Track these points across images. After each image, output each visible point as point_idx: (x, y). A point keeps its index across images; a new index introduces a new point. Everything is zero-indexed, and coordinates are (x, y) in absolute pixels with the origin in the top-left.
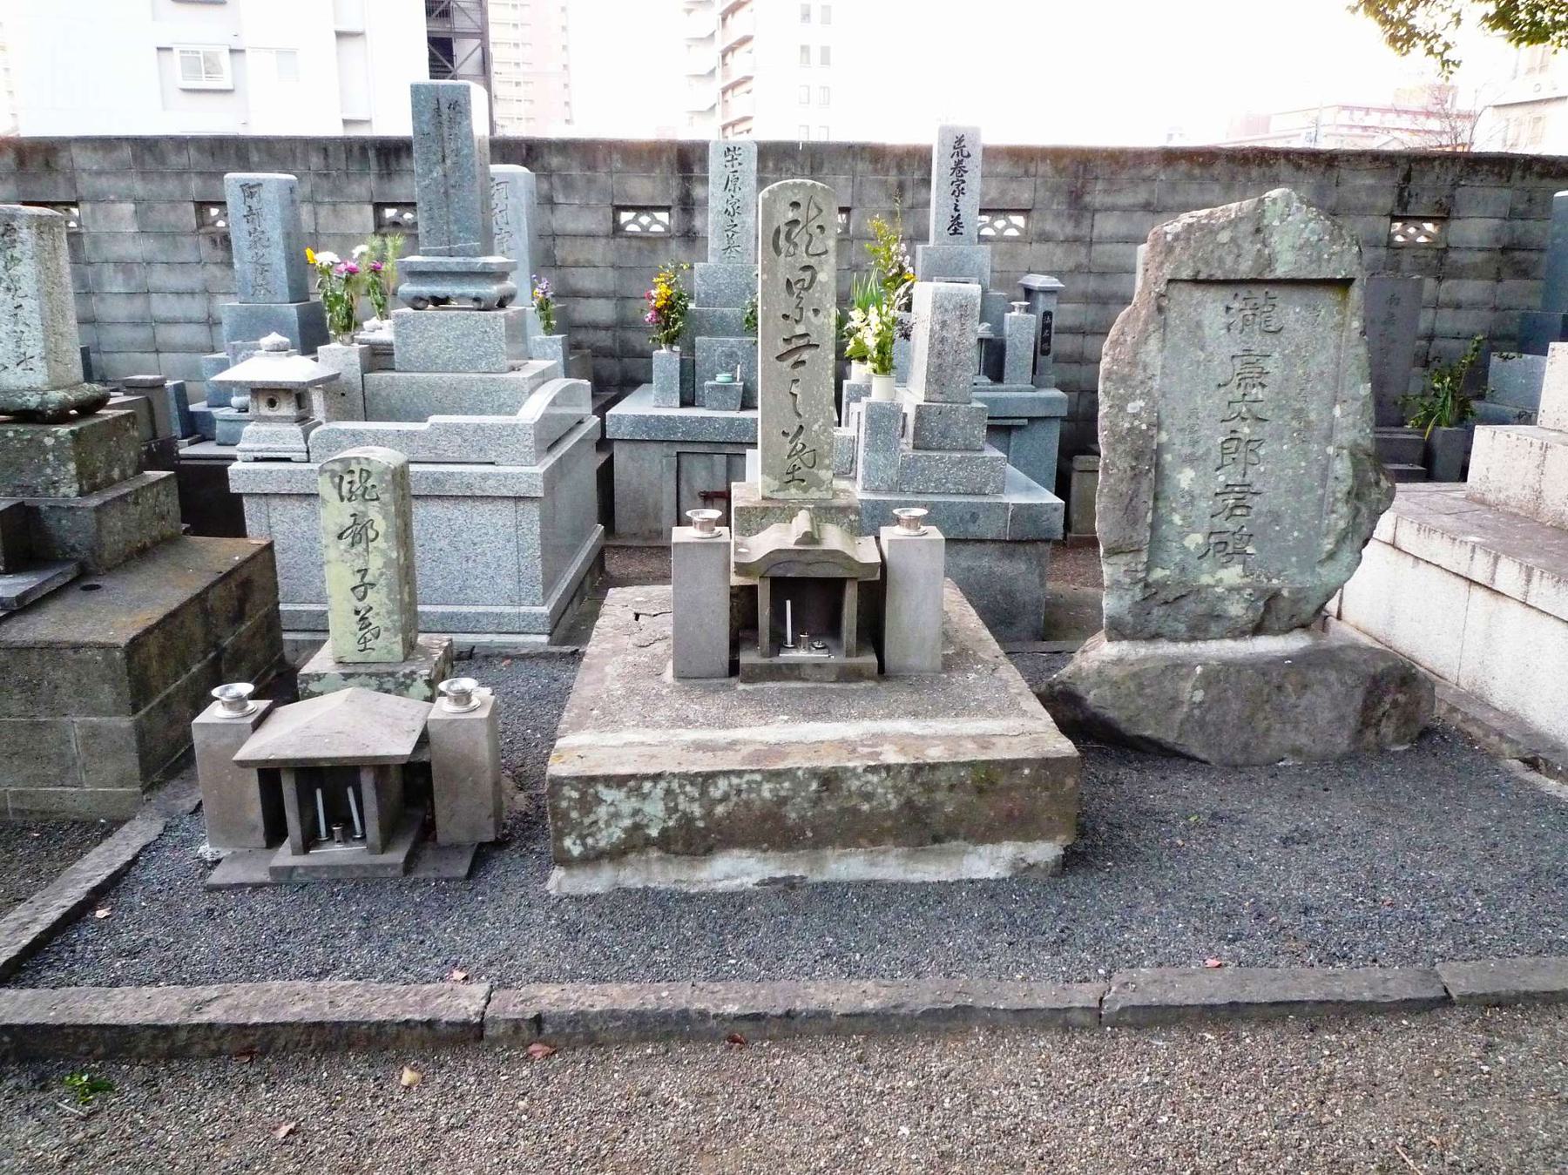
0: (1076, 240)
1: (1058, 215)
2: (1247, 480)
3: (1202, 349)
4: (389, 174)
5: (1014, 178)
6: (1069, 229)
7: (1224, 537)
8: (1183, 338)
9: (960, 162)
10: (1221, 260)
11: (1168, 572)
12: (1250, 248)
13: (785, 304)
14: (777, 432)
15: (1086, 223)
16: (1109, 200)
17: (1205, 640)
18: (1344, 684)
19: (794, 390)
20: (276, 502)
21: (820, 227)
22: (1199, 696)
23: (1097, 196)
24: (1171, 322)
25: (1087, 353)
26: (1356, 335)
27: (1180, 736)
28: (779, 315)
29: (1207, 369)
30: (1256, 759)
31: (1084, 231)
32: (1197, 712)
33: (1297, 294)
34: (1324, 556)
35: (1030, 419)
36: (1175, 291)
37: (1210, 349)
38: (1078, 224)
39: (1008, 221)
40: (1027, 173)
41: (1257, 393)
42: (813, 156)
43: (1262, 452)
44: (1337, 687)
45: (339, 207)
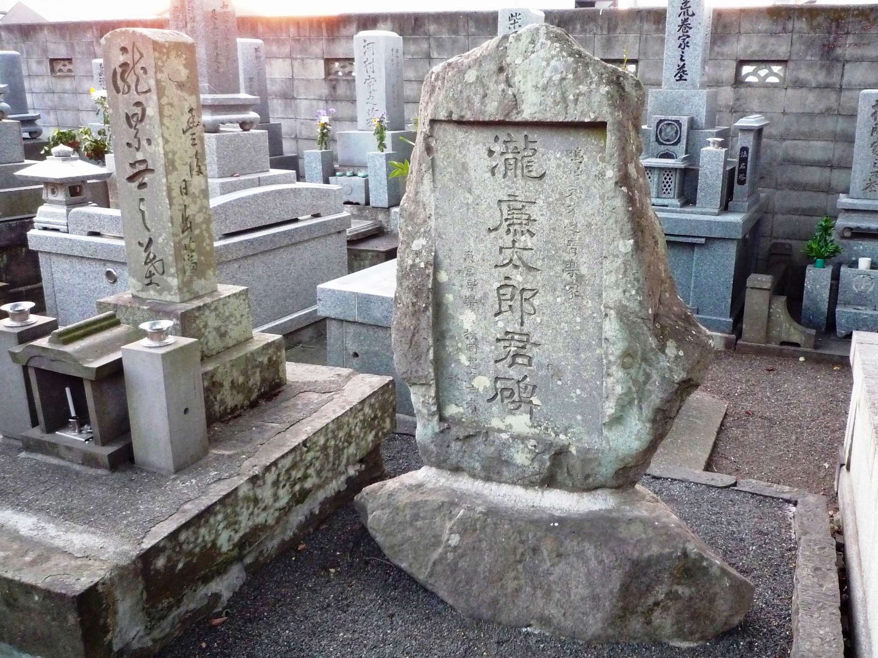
0: (827, 86)
1: (811, 65)
2: (525, 329)
3: (470, 191)
4: (333, 39)
5: (773, 34)
6: (822, 77)
7: (509, 384)
8: (451, 180)
9: (686, 20)
10: (469, 101)
11: (461, 410)
12: (496, 88)
13: (127, 134)
14: (135, 242)
15: (836, 73)
16: (859, 52)
17: (500, 482)
18: (601, 562)
19: (142, 207)
20: (54, 258)
21: (143, 68)
22: (455, 540)
23: (847, 49)
24: (438, 162)
25: (834, 183)
26: (610, 184)
27: (431, 575)
28: (125, 141)
29: (476, 212)
30: (504, 618)
31: (835, 79)
32: (450, 556)
33: (557, 139)
34: (606, 420)
35: (707, 238)
36: (439, 130)
37: (477, 192)
38: (829, 72)
39: (770, 70)
40: (785, 30)
41: (525, 240)
42: (610, 19)
43: (536, 302)
44: (593, 563)
45: (306, 61)
